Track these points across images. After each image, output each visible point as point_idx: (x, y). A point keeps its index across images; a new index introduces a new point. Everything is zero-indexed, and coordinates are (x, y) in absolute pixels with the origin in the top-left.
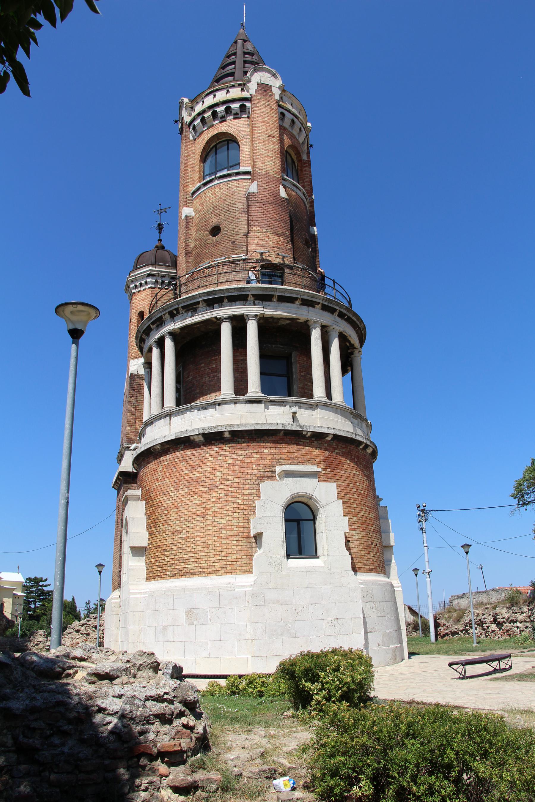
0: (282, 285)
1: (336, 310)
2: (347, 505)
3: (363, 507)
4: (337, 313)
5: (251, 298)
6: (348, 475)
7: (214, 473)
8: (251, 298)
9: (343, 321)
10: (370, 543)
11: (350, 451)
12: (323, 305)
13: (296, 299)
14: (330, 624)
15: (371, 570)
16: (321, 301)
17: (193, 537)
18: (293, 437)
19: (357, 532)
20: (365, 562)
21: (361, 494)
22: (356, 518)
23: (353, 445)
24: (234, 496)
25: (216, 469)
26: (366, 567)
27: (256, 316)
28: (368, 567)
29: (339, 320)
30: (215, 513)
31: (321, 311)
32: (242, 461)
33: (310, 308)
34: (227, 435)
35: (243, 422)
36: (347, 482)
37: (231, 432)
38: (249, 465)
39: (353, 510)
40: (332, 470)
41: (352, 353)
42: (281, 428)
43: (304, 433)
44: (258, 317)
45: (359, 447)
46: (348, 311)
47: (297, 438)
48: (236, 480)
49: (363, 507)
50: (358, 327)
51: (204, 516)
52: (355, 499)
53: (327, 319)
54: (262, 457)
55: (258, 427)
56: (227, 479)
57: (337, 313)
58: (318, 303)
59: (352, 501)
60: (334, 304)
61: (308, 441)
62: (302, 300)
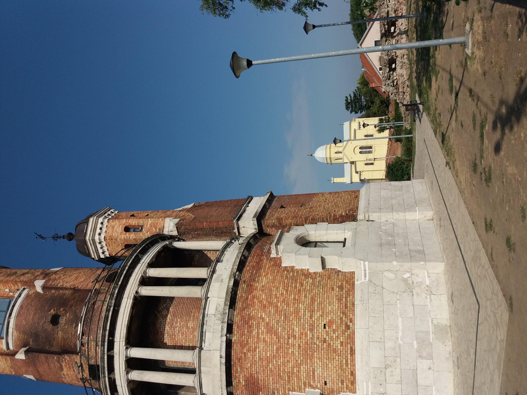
2: (291, 378)
3: (290, 352)
6: (262, 368)
15: (352, 352)
19: (316, 368)
20: (344, 360)
22: (302, 367)
26: (349, 363)
28: (349, 357)
36: (269, 371)
39: (295, 369)
49: (290, 350)
52: (284, 364)
59: (286, 370)
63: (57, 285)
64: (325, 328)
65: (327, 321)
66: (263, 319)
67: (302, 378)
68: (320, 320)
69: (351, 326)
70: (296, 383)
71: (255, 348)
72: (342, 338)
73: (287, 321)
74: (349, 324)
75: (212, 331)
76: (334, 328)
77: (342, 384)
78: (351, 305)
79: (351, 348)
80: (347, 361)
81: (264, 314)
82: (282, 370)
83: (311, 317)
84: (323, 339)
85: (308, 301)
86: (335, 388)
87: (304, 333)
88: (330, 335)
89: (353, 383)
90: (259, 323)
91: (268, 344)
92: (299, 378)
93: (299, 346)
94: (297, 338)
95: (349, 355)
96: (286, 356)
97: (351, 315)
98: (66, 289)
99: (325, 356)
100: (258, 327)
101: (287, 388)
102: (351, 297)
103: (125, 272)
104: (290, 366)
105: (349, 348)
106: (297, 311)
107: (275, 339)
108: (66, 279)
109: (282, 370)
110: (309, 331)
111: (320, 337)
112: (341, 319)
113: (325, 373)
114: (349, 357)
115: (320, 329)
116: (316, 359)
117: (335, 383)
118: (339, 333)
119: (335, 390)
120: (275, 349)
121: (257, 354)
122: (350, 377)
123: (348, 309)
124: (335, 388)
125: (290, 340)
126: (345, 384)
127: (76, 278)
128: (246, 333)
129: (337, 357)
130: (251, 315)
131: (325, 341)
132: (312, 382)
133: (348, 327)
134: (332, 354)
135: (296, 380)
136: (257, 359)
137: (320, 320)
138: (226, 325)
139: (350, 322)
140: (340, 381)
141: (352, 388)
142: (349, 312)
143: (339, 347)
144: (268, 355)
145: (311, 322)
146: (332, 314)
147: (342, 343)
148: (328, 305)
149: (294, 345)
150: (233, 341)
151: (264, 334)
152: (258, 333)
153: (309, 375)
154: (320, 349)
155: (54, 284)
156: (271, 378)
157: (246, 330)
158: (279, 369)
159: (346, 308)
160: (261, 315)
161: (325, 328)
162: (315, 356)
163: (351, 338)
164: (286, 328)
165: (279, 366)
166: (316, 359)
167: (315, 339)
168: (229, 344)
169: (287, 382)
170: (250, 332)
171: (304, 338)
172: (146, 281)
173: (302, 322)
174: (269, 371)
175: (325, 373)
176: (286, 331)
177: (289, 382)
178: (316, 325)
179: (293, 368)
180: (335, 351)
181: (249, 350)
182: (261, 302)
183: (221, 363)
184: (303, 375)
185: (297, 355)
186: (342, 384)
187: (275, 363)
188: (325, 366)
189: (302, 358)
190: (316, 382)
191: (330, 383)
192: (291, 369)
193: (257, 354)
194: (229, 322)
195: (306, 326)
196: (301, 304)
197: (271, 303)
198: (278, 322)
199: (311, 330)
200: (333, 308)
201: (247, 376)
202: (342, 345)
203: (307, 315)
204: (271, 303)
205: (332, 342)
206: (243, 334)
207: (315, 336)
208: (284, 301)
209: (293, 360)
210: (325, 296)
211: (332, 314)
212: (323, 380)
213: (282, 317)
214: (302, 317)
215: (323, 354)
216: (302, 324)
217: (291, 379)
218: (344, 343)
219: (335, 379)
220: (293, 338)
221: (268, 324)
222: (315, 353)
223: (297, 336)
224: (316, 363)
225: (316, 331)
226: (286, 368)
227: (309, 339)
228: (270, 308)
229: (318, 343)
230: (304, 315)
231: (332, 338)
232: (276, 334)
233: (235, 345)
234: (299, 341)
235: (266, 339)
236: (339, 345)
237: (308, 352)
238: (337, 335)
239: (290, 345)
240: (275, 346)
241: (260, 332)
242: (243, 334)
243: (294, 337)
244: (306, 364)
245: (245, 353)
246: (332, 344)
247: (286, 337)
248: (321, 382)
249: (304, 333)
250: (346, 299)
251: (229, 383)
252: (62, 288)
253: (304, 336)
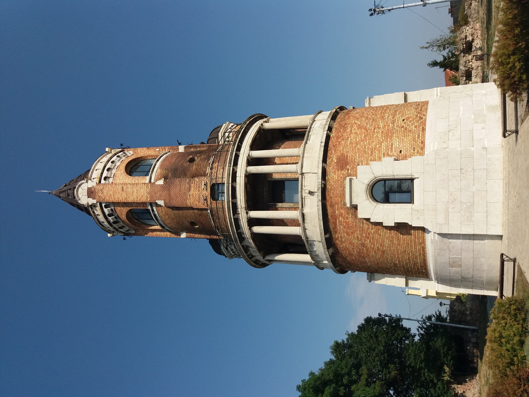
0: (224, 193)
1: (236, 154)
5: (236, 216)
7: (354, 244)
8: (236, 216)
11: (334, 146)
13: (232, 186)
17: (398, 257)
21: (365, 136)
24: (369, 234)
25: (350, 243)
27: (247, 213)
30: (381, 246)
32: (345, 227)
34: (327, 236)
35: (318, 225)
37: (325, 234)
38: (347, 223)
40: (347, 164)
42: (320, 203)
48: (358, 232)
51: (384, 252)
52: (369, 144)
54: (341, 215)
56: (358, 237)
60: (232, 156)
62: (232, 182)
83: (393, 118)
93: (382, 132)
100: (352, 126)
106: (383, 118)
125: (376, 131)
158: (365, 147)
168: (328, 138)
183: (321, 146)
198: (367, 123)
199: (393, 123)
206: (340, 132)
230: (388, 116)
232: (365, 128)
242: (340, 132)
243: (379, 128)
251: (325, 160)
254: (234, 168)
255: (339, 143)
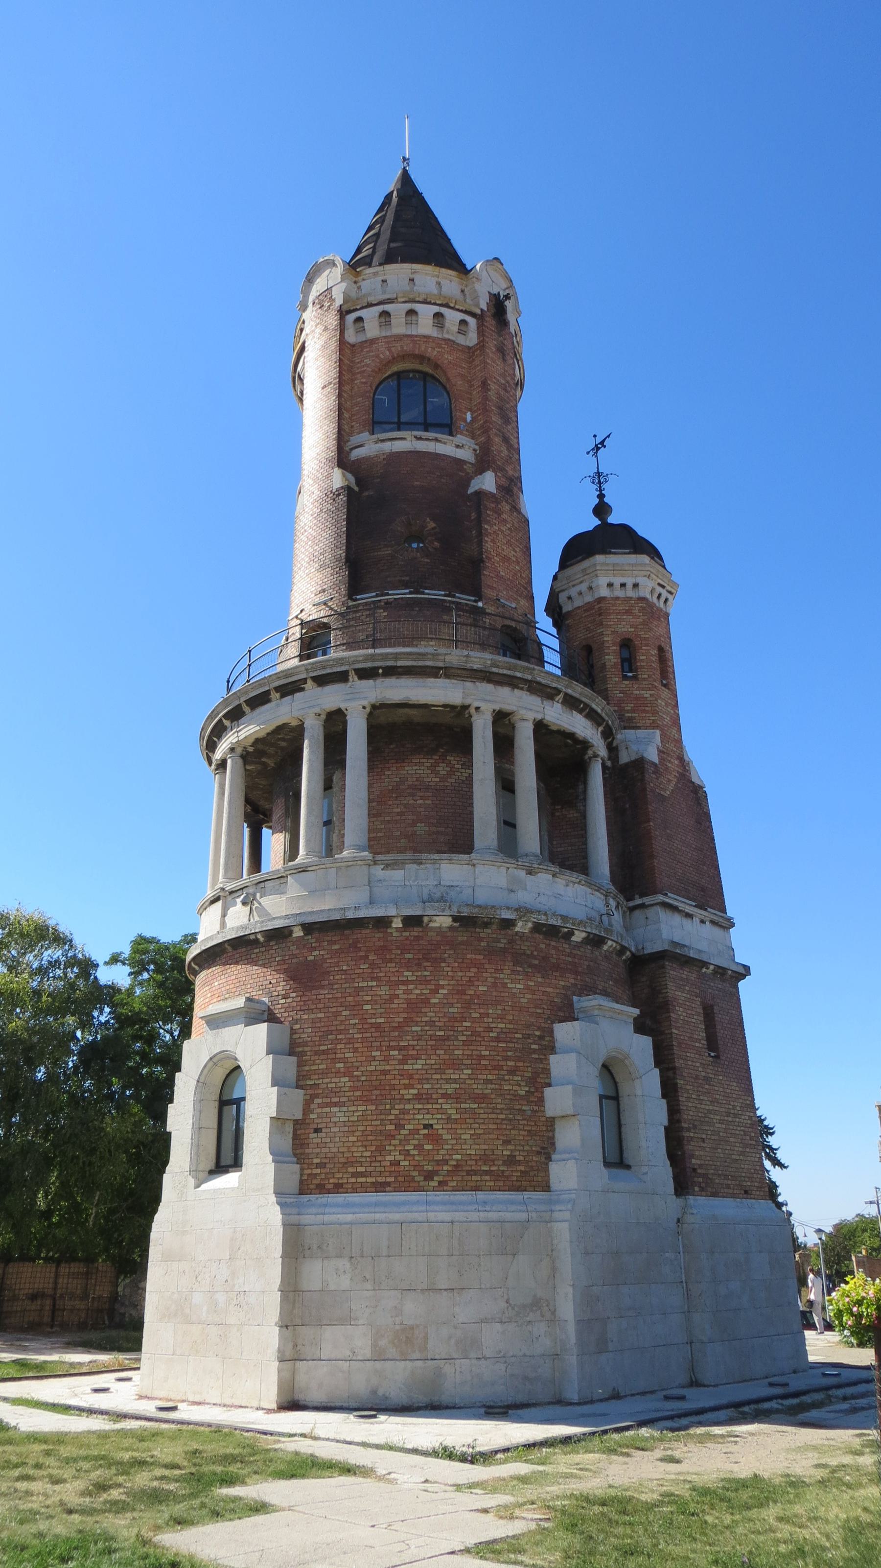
2: (325, 1057)
3: (374, 1054)
4: (352, 676)
5: (227, 723)
6: (339, 995)
9: (379, 681)
10: (393, 1127)
12: (314, 679)
13: (268, 693)
14: (235, 1302)
15: (380, 1187)
16: (303, 676)
18: (244, 949)
19: (345, 1109)
20: (362, 1169)
21: (377, 1026)
22: (347, 1079)
23: (367, 928)
27: (232, 750)
28: (370, 1180)
29: (367, 684)
31: (320, 689)
33: (298, 695)
36: (334, 1010)
39: (342, 1065)
41: (471, 716)
43: (252, 937)
44: (239, 750)
45: (390, 927)
46: (373, 661)
47: (249, 948)
49: (378, 1053)
50: (441, 668)
52: (350, 1041)
53: (331, 697)
55: (204, 948)
57: (352, 676)
58: (305, 681)
59: (339, 1047)
61: (264, 949)
62: (277, 689)
63: (488, 522)
64: (426, 1126)
65: (440, 1132)
66: (435, 991)
67: (326, 1081)
68: (439, 1116)
69: (433, 1184)
70: (315, 1067)
71: (377, 979)
72: (407, 1163)
73: (433, 1043)
74: (436, 1178)
75: (407, 883)
76: (426, 1147)
77: (318, 1166)
78: (474, 1184)
79: (388, 1184)
80: (362, 1175)
81: (445, 992)
82: (339, 1037)
83: (445, 1096)
84: (402, 1122)
85: (478, 1088)
86: (309, 1151)
87: (412, 1082)
88: (411, 1137)
89: (321, 1189)
90: (427, 982)
91: (387, 1006)
92: (324, 1073)
93: (384, 1073)
94: (401, 1067)
95: (373, 1180)
96: (365, 1045)
97: (454, 1184)
98: (480, 544)
99: (369, 1128)
101: (306, 1049)
102: (492, 1184)
103: (519, 675)
104: (347, 1055)
105: (388, 1180)
106: (455, 1065)
107: (397, 1020)
108: (501, 537)
109: (339, 1037)
110: (415, 1092)
111: (406, 1117)
112: (446, 1162)
113: (337, 1130)
114: (370, 1180)
115: (421, 1117)
116: (364, 1108)
117: (318, 1150)
118: (417, 1158)
119: (307, 1151)
120: (379, 1020)
121: (365, 984)
122: (331, 1181)
123: (466, 1178)
124: (309, 1151)
125: (396, 1052)
126: (318, 1171)
127: (506, 559)
128: (407, 956)
129: (368, 1154)
130: (443, 965)
131: (399, 1126)
132: (319, 1101)
133: (429, 1176)
134: (374, 1143)
135: (321, 1067)
136: (356, 985)
137: (439, 1116)
138: (419, 913)
139: (440, 1182)
140: (324, 1161)
141: (312, 1187)
142: (460, 1178)
143: (388, 1158)
144: (366, 1007)
145: (434, 1096)
146: (454, 1142)
147: (397, 1163)
148: (472, 1132)
149: (387, 1059)
150: (389, 930)
151: (405, 996)
152: (406, 983)
153: (332, 1095)
154: (383, 1117)
155: (489, 515)
156: (322, 1015)
157: (410, 956)
158: (340, 1032)
159: (469, 1173)
160: (443, 987)
161: (426, 1126)
162: (369, 1107)
163: (406, 1184)
164: (421, 1043)
165: (345, 1031)
166: (364, 1108)
167: (402, 1106)
169: (317, 1049)
170: (408, 965)
171: (403, 1082)
172: (503, 722)
173: (435, 1076)
174: (334, 1010)
175: (337, 1130)
176: (415, 1043)
177: (316, 1053)
178: (430, 1106)
179: (344, 1060)
180: (381, 1149)
181: (373, 965)
182: (470, 981)
183: (344, 909)
184: (331, 1082)
185: (369, 1068)
186: (318, 1166)
187: (352, 1022)
188: (351, 1129)
189: (363, 1078)
190: (319, 1110)
191: (319, 1141)
192: (342, 1056)
193: (365, 984)
194: (426, 919)
195: (426, 1086)
196: (470, 1072)
197: (468, 1005)
198: (431, 1023)
199: (418, 1098)
200: (465, 1144)
201: (325, 965)
202: (392, 1163)
203: (448, 1086)
204: (468, 1005)
205: (397, 1142)
207: (407, 1107)
208: (474, 1033)
209: (360, 1059)
210: (491, 1126)
211: (454, 1142)
212: (324, 1125)
213: (442, 1033)
214: (444, 1076)
215: (374, 1123)
216: (429, 1076)
217: (322, 1057)
218: (397, 1168)
219: (327, 1150)
220: (401, 1057)
221: (426, 1002)
222: (374, 1107)
223: (406, 1067)
224: (354, 1108)
225: (417, 1106)
226: (342, 1046)
227: (402, 1092)
228: (459, 1005)
229: (393, 1112)
230: (448, 1081)
231: (405, 1141)
233: (381, 935)
234: (396, 1072)
235: (396, 1001)
236: (392, 1158)
237: (376, 1091)
238: (412, 1152)
239: (386, 1053)
240: (382, 1020)
241: (411, 987)
242: (404, 950)
243: (404, 1061)
244: (353, 1089)
245: (367, 957)
246: (393, 1142)
247: (401, 1044)
248: (320, 1121)
249: (412, 1082)
250: (486, 1173)
251: (308, 928)
252: (480, 534)
253: (407, 1082)
254: (309, 682)
255: (361, 958)
